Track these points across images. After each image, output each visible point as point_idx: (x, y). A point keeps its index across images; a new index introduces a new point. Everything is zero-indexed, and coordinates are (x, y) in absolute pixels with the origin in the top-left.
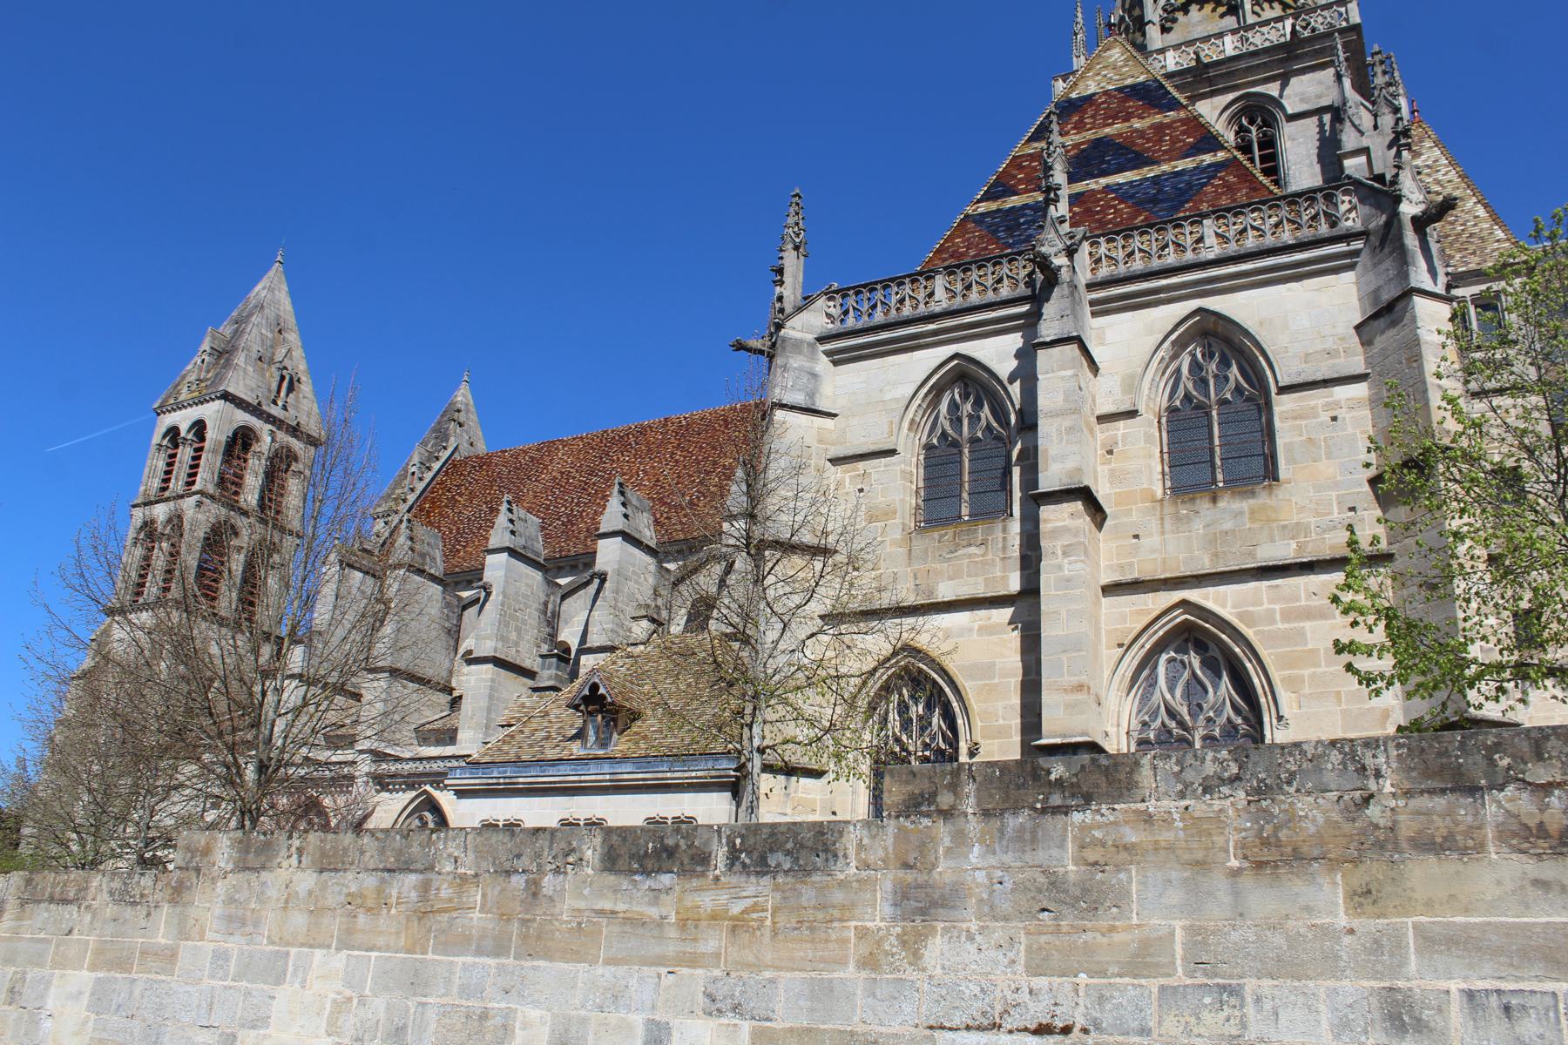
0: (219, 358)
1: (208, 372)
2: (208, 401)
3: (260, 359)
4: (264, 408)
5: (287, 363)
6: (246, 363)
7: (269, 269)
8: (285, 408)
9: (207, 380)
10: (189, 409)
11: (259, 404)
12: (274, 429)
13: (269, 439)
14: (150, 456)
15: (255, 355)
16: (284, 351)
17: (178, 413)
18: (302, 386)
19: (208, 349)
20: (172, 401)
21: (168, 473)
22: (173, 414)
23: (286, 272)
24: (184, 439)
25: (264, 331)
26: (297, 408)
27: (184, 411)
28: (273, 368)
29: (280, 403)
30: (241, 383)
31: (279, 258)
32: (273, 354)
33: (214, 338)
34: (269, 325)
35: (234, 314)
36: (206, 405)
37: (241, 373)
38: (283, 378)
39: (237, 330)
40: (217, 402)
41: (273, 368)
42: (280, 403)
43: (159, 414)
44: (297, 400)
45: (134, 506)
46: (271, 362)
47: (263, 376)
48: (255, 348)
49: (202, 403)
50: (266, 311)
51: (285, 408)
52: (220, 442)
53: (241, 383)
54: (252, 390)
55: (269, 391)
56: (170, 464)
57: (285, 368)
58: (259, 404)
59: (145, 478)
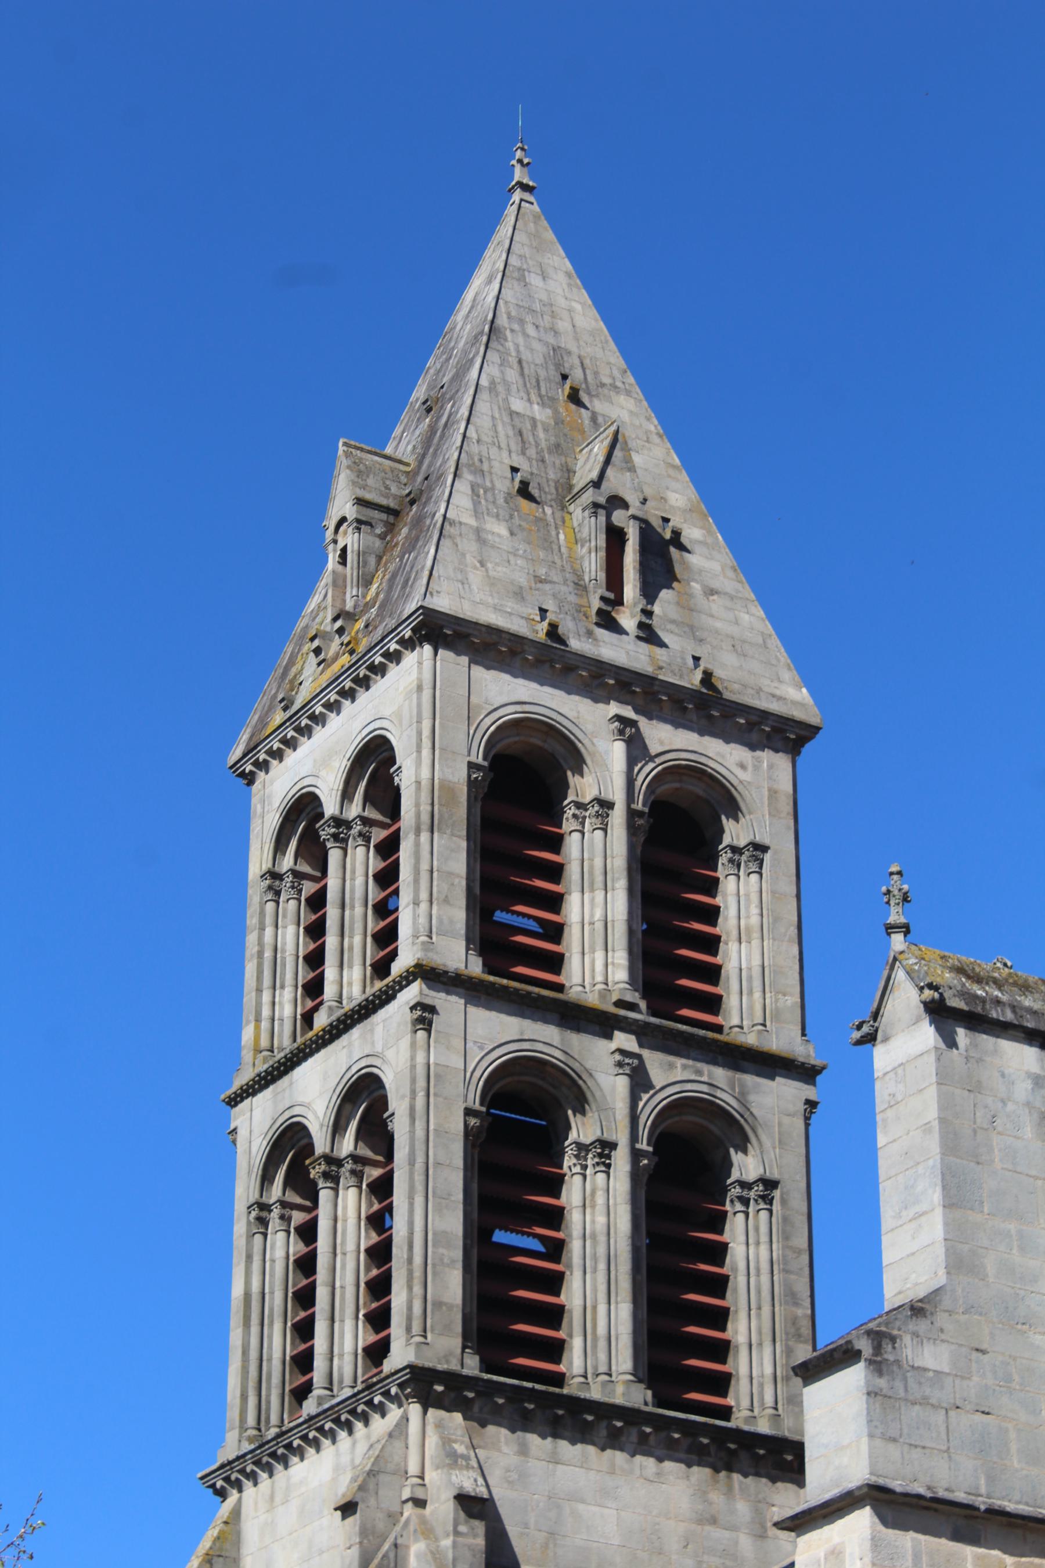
0: (391, 528)
1: (366, 582)
2: (380, 670)
3: (524, 491)
4: (576, 644)
5: (617, 482)
6: (477, 513)
7: (497, 219)
8: (648, 634)
9: (368, 606)
10: (334, 721)
11: (553, 632)
12: (628, 712)
13: (618, 751)
14: (252, 921)
15: (504, 485)
16: (599, 449)
17: (306, 747)
18: (694, 560)
19: (350, 511)
20: (279, 717)
21: (315, 959)
22: (292, 758)
23: (549, 213)
24: (338, 822)
25: (518, 405)
26: (692, 630)
27: (320, 734)
28: (578, 513)
29: (628, 620)
30: (476, 578)
31: (519, 174)
32: (569, 472)
33: (360, 472)
34: (532, 385)
35: (419, 393)
36: (380, 686)
37: (469, 546)
38: (615, 538)
39: (432, 429)
40: (410, 659)
41: (578, 513)
42: (628, 620)
43: (250, 779)
44: (686, 605)
45: (234, 1101)
46: (566, 494)
47: (548, 544)
48: (500, 462)
49: (364, 683)
50: (512, 341)
51: (648, 634)
52: (447, 789)
53: (476, 578)
54: (519, 595)
55: (580, 587)
56: (316, 930)
57: (617, 502)
58: (553, 632)
59: (249, 998)
